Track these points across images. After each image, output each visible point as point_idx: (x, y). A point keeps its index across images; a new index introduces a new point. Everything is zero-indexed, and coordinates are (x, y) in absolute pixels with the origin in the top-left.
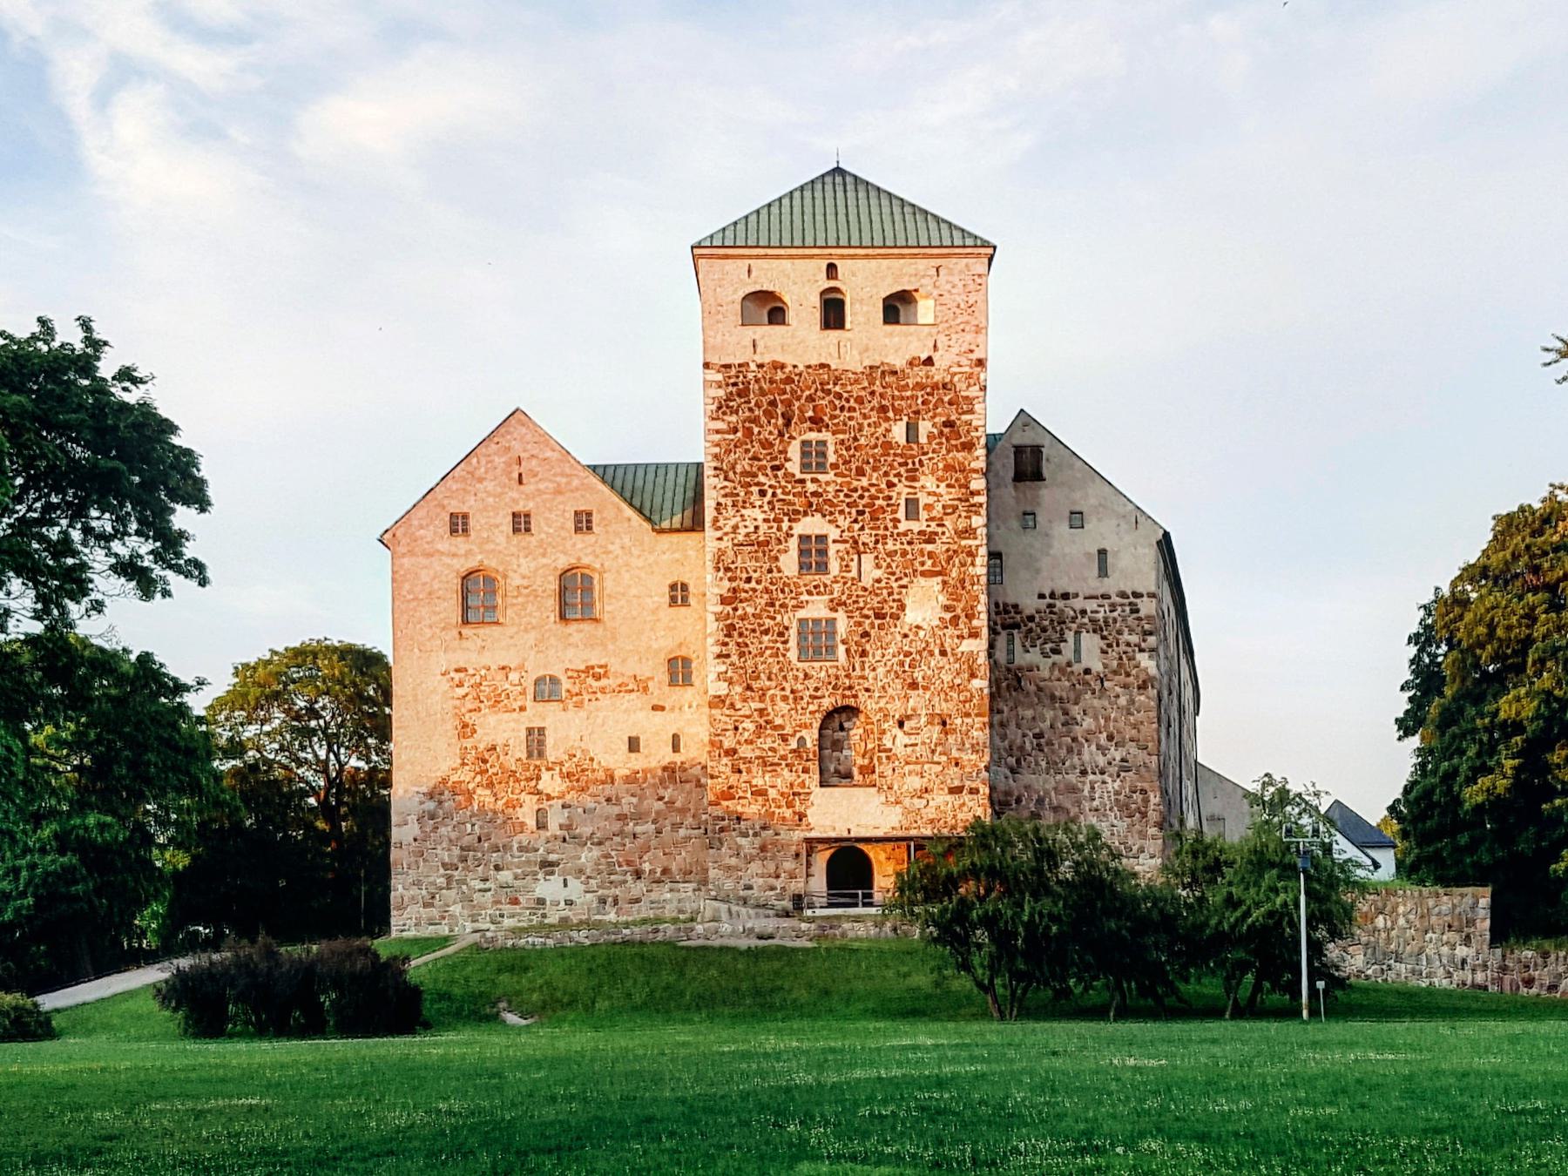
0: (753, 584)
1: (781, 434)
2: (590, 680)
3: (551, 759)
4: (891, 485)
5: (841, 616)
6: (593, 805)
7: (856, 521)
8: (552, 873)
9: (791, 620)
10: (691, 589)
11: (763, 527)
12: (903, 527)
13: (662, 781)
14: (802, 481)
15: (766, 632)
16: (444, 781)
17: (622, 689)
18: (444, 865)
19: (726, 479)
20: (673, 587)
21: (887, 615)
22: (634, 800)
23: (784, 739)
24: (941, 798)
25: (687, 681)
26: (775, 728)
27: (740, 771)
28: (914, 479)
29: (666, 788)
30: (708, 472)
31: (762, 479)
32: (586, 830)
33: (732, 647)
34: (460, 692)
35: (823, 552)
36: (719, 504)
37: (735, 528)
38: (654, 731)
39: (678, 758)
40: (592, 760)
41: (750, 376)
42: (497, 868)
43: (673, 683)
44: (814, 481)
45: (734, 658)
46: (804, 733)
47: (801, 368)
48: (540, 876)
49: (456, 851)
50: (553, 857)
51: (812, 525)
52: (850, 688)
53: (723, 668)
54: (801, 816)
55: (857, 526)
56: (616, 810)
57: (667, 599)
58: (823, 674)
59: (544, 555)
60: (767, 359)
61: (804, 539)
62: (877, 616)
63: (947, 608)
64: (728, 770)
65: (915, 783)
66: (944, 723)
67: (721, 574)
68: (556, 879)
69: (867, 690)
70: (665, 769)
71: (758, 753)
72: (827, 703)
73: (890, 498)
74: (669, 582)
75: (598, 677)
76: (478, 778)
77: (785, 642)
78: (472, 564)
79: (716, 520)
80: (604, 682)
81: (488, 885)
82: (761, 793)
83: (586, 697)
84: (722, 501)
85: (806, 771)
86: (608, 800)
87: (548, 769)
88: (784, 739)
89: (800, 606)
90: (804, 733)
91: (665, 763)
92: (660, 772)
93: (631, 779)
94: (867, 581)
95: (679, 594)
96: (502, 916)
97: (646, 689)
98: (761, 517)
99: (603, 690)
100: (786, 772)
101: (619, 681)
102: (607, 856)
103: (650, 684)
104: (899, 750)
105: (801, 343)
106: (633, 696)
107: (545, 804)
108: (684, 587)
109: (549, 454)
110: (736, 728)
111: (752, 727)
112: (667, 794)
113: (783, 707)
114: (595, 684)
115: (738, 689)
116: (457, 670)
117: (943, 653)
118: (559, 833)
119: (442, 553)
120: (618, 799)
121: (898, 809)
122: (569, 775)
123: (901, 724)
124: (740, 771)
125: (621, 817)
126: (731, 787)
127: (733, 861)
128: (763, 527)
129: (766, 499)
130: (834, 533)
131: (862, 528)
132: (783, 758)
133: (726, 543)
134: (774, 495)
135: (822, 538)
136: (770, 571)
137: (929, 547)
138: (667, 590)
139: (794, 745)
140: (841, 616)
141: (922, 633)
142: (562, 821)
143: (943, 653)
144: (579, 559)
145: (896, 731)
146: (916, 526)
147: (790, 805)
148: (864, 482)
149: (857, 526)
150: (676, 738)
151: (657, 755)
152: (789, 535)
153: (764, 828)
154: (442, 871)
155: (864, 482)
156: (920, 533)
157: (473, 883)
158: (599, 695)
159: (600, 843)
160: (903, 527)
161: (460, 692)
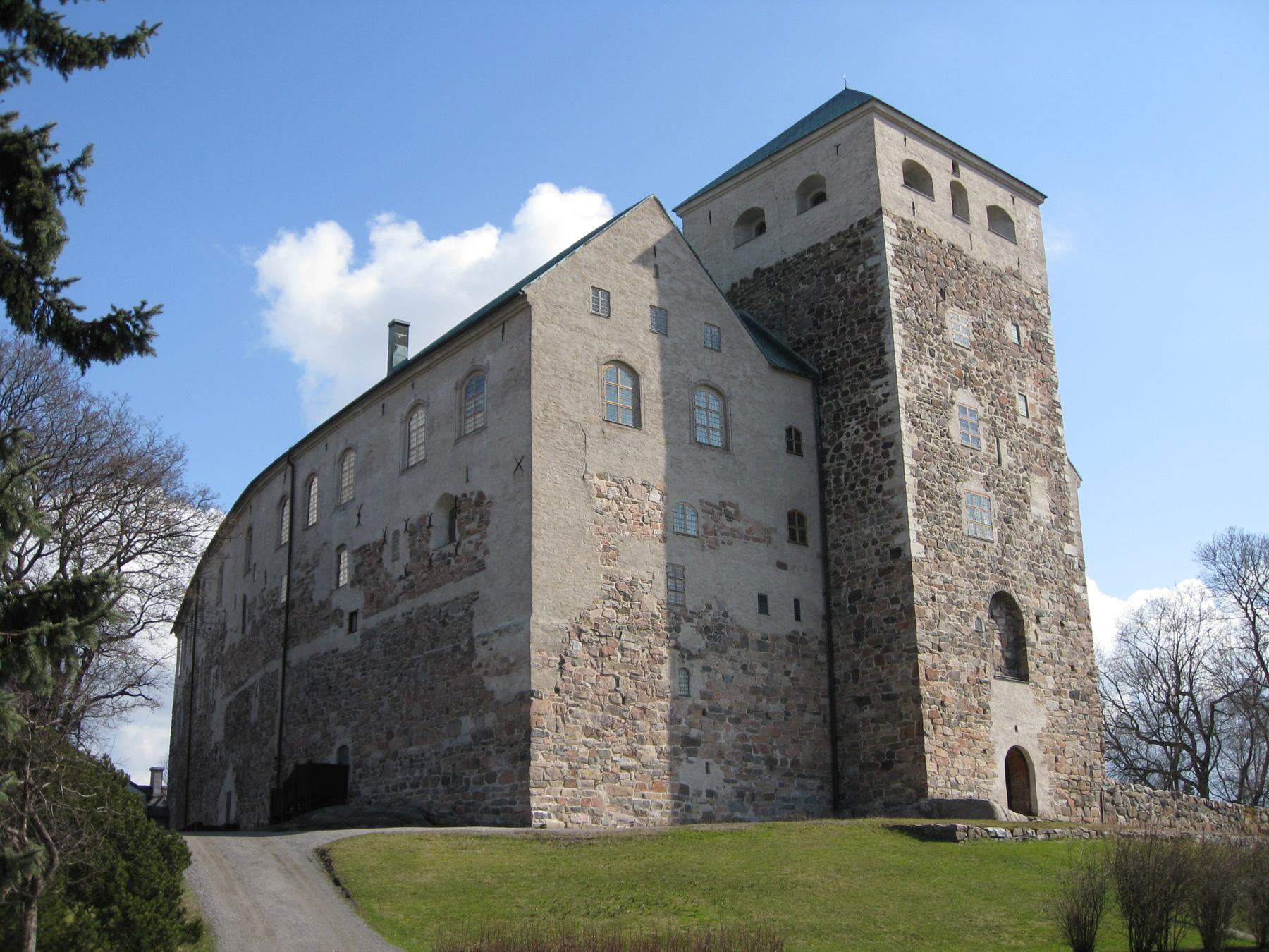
0: (932, 444)
1: (937, 301)
2: (723, 518)
3: (690, 607)
4: (1009, 379)
5: (990, 493)
6: (731, 672)
7: (992, 404)
8: (693, 753)
9: (962, 488)
10: (804, 438)
11: (935, 386)
12: (1021, 420)
13: (787, 653)
14: (954, 352)
15: (944, 498)
16: (584, 617)
17: (748, 536)
18: (586, 728)
19: (906, 328)
20: (789, 431)
21: (1020, 502)
22: (766, 671)
23: (965, 617)
24: (1067, 700)
25: (803, 541)
26: (957, 605)
27: (940, 650)
28: (1022, 377)
29: (791, 661)
30: (894, 316)
31: (929, 338)
32: (724, 703)
33: (923, 507)
34: (601, 503)
35: (975, 427)
36: (904, 352)
37: (916, 383)
38: (783, 588)
39: (800, 628)
40: (725, 615)
41: (914, 235)
42: (641, 740)
43: (792, 538)
44: (963, 354)
45: (924, 520)
46: (979, 614)
47: (944, 242)
48: (683, 756)
49: (600, 714)
50: (694, 733)
51: (963, 397)
52: (1004, 573)
53: (920, 529)
54: (986, 709)
55: (994, 409)
56: (750, 681)
57: (784, 444)
58: (985, 553)
59: (678, 363)
60: (923, 225)
61: (963, 409)
62: (1017, 505)
63: (1053, 510)
64: (929, 645)
65: (1050, 682)
66: (1062, 625)
67: (909, 424)
68: (699, 761)
69: (1014, 578)
70: (790, 638)
71: (950, 631)
72: (990, 585)
73: (1009, 390)
74: (785, 426)
75: (730, 519)
76: (623, 619)
77: (959, 513)
78: (613, 350)
79: (903, 366)
80: (736, 524)
81: (631, 762)
82: (955, 678)
83: (720, 538)
84: (906, 349)
85: (984, 657)
86: (744, 667)
87: (689, 620)
88: (965, 617)
89: (967, 477)
90: (979, 614)
91: (788, 631)
92: (786, 642)
93: (762, 645)
94: (1005, 466)
95: (793, 440)
96: (645, 804)
97: (770, 541)
98: (933, 375)
99: (734, 533)
100: (971, 657)
101: (748, 526)
102: (743, 738)
103: (774, 536)
104: (1039, 645)
105: (934, 216)
106: (762, 546)
107: (687, 664)
108: (798, 434)
109: (681, 255)
110: (933, 599)
111: (944, 598)
112: (793, 667)
113: (962, 582)
114: (728, 524)
115: (932, 554)
116: (600, 476)
117: (1054, 553)
118: (700, 702)
119: (582, 330)
120: (752, 667)
121: (1043, 709)
122: (706, 630)
123: (1038, 618)
124: (940, 650)
125: (755, 690)
126: (934, 666)
127: (943, 753)
128: (935, 386)
129: (935, 360)
130: (981, 412)
131: (996, 413)
132: (967, 639)
133: (912, 395)
134: (940, 358)
135: (974, 413)
136: (942, 435)
137: (1037, 446)
138: (784, 434)
139: (973, 627)
140: (990, 493)
141: (1041, 529)
142: (703, 687)
143: (1054, 553)
144: (709, 375)
145: (1034, 626)
146: (1029, 424)
147: (977, 694)
148: (993, 367)
149: (994, 409)
150: (797, 603)
151: (781, 622)
152: (953, 403)
153: (961, 717)
154: (584, 738)
155: (993, 367)
156: (1031, 430)
157: (617, 757)
158: (730, 538)
159: (736, 721)
160: (1021, 420)
161: (601, 503)
